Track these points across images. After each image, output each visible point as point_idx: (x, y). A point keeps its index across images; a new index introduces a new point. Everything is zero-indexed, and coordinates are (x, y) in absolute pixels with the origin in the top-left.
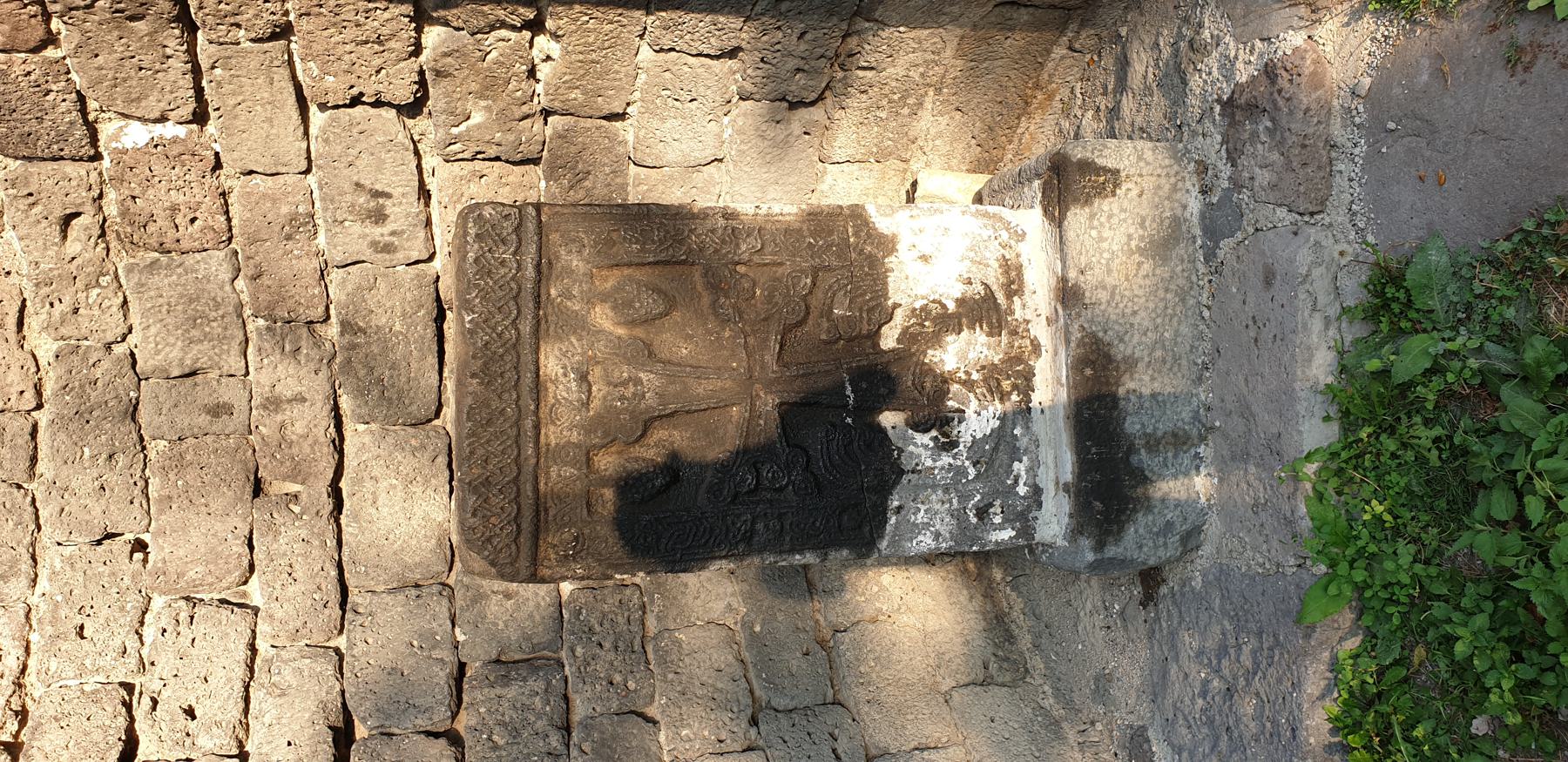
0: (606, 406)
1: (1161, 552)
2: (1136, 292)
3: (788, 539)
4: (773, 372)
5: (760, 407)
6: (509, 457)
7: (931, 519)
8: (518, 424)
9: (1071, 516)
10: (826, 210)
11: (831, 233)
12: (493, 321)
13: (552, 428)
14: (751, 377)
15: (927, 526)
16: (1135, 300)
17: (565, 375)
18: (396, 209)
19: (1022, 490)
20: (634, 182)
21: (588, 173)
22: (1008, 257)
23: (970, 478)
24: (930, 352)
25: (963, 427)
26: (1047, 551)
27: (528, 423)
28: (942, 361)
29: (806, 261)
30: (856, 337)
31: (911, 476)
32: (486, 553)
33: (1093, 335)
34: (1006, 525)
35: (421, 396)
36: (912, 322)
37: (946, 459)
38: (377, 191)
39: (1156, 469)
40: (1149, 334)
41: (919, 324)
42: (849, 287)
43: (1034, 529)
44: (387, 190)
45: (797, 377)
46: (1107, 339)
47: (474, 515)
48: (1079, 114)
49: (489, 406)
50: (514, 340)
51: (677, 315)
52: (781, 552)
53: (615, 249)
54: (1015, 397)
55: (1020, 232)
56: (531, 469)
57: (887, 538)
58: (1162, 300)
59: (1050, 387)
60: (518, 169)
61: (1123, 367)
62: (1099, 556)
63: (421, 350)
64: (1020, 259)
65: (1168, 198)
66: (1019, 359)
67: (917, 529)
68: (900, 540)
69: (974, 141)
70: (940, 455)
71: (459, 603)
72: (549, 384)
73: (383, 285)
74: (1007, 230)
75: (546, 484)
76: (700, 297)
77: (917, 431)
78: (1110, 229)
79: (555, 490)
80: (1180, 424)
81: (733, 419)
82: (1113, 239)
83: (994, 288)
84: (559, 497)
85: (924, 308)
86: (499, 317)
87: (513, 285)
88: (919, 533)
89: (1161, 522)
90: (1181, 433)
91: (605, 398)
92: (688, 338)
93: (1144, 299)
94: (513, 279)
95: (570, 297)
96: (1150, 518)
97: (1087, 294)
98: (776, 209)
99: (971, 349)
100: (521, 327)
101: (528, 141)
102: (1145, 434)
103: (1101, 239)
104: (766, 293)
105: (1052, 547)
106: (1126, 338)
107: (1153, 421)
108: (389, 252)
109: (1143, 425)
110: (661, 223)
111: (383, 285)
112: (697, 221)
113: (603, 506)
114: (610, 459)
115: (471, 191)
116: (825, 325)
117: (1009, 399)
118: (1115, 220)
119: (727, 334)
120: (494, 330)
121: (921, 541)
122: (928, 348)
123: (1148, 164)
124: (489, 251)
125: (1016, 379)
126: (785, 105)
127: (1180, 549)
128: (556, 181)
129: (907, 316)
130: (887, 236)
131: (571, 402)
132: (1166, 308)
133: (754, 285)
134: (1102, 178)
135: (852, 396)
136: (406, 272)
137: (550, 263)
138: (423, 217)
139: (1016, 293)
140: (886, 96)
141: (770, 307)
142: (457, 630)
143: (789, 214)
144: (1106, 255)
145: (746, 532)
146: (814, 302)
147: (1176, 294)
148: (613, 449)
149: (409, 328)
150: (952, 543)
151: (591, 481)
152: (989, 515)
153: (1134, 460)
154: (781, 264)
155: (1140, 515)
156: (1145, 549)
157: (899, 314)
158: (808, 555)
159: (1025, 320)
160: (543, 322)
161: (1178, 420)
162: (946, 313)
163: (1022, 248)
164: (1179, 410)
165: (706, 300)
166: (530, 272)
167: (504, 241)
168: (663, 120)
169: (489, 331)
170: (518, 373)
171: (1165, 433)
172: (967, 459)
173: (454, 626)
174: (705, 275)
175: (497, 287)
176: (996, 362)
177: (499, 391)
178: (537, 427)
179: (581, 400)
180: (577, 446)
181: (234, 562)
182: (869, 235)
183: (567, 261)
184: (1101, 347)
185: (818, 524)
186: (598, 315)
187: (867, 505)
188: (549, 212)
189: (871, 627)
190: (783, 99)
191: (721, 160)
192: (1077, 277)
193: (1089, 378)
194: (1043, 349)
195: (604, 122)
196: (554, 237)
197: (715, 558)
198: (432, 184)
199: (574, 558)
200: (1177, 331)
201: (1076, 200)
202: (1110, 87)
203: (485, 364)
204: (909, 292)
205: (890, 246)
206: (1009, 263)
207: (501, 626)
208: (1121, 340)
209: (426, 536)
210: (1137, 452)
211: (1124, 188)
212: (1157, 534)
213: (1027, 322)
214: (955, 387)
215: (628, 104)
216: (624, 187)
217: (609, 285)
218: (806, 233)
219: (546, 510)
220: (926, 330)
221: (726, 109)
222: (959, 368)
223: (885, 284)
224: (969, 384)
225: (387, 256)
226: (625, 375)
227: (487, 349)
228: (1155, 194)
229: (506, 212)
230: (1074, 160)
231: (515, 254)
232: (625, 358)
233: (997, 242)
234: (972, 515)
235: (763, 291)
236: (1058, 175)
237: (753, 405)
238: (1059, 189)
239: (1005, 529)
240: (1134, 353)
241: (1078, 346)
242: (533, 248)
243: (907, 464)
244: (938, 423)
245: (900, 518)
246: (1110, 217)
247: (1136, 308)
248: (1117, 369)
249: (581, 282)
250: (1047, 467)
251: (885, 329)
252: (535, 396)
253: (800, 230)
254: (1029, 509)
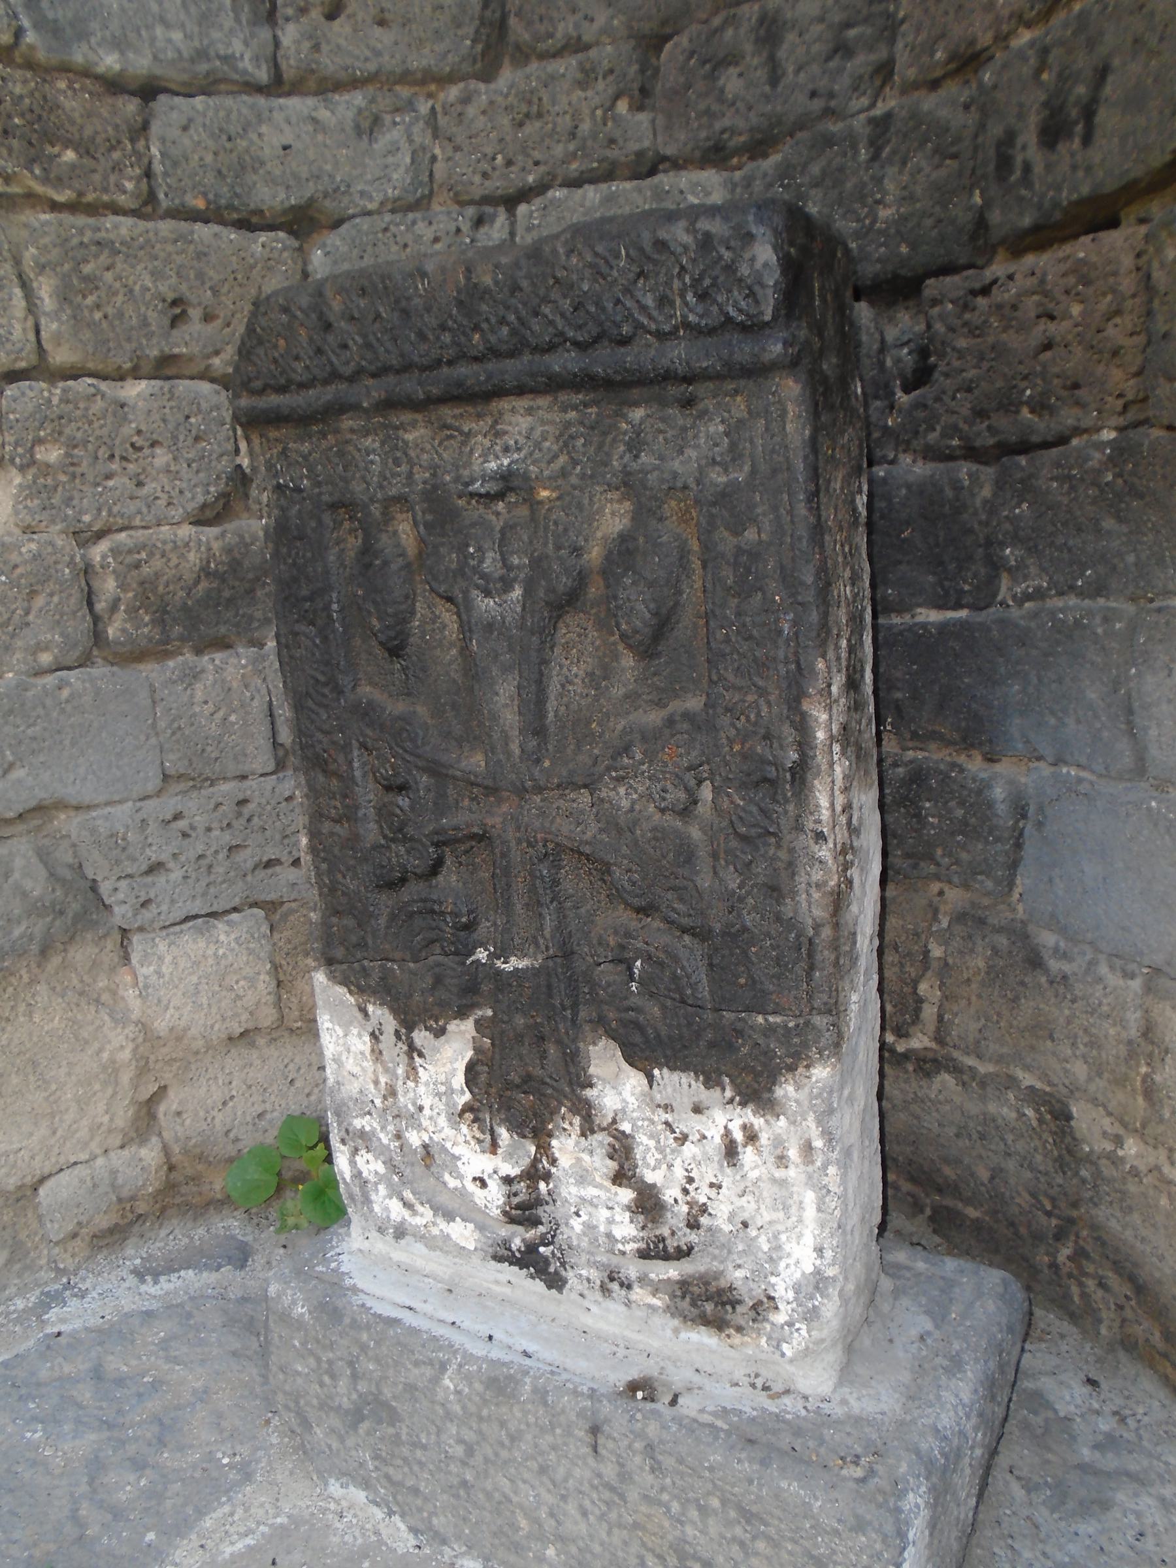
86: (566, 304)
94: (639, 326)
103: (703, 1510)
108: (999, 168)
120: (546, 300)
128: (1110, 458)
135: (508, 967)
144: (675, 1507)
179: (473, 481)
181: (542, 28)
231: (686, 325)
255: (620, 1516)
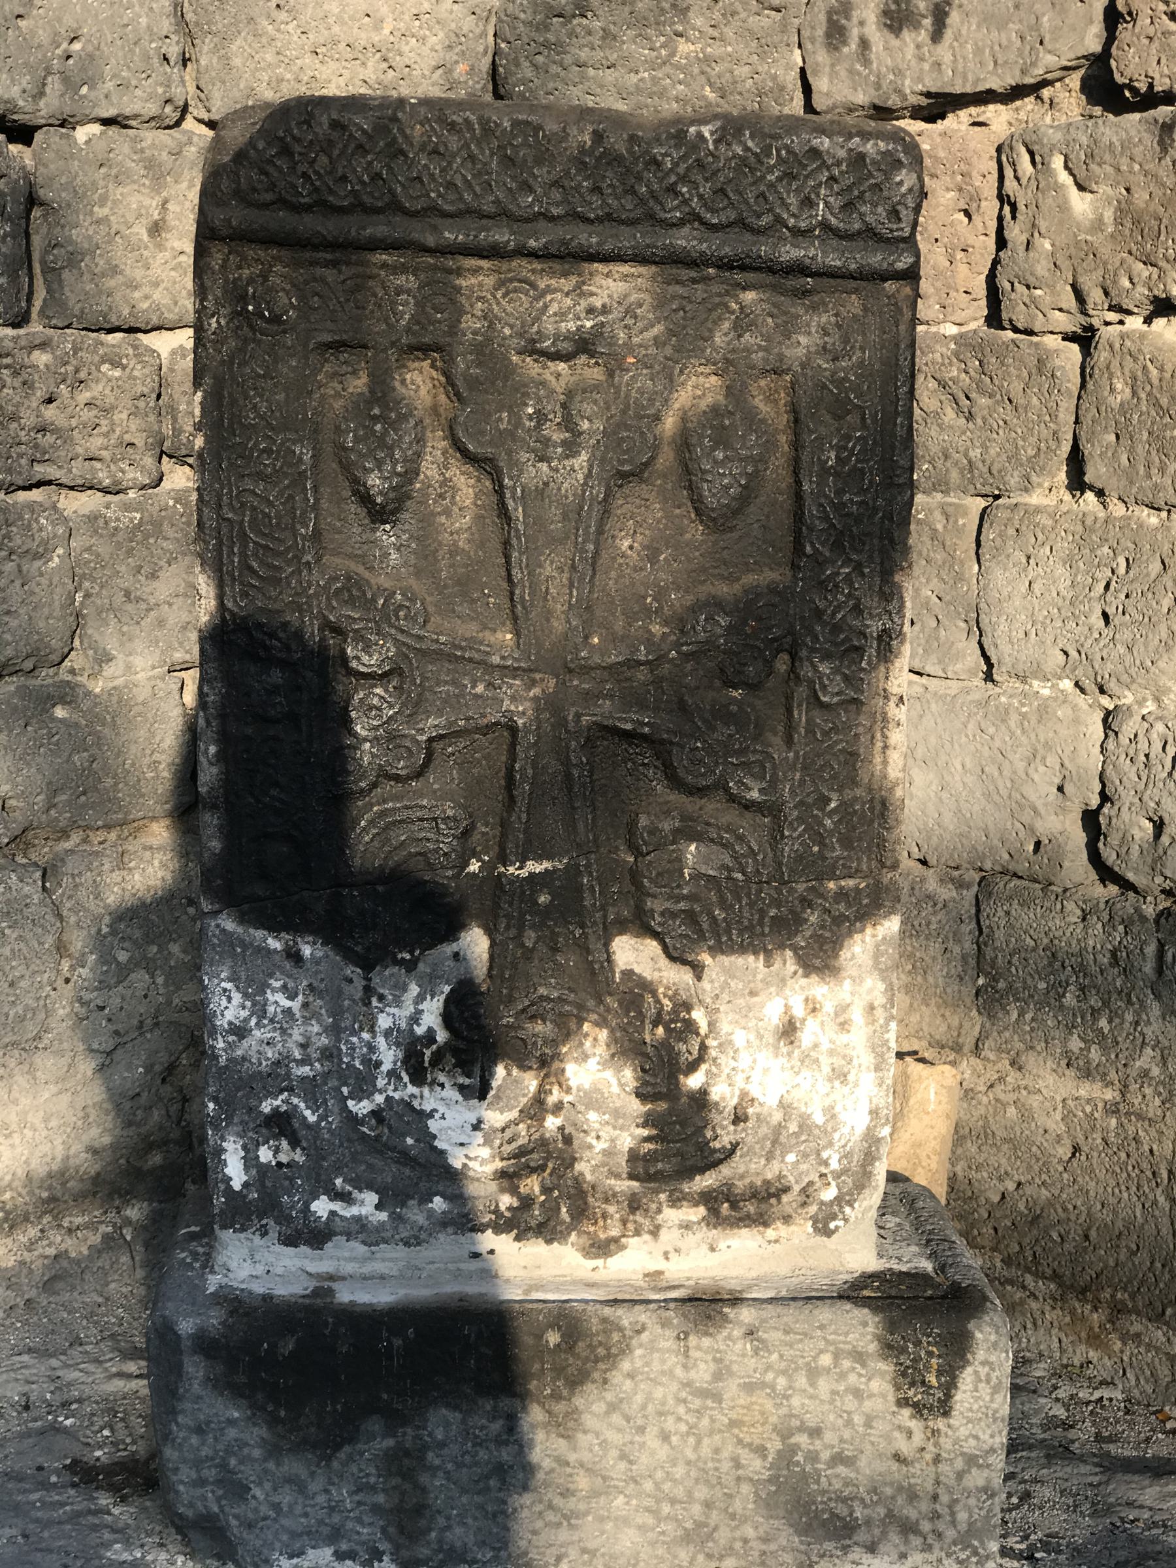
0: (526, 385)
1: (186, 1473)
2: (706, 1441)
3: (249, 731)
4: (578, 716)
5: (511, 686)
6: (440, 195)
7: (272, 1021)
8: (503, 215)
9: (267, 1298)
10: (892, 837)
11: (846, 843)
12: (699, 178)
13: (490, 281)
14: (570, 671)
15: (260, 1011)
16: (692, 1440)
17: (590, 311)
18: (910, 51)
19: (322, 1207)
20: (950, 504)
21: (970, 417)
22: (785, 1199)
23: (350, 1103)
24: (603, 1035)
25: (451, 1093)
26: (197, 1260)
27: (503, 236)
28: (585, 1057)
29: (792, 791)
30: (639, 886)
31: (359, 983)
32: (261, 145)
33: (626, 1350)
34: (254, 1172)
35: (551, 85)
36: (666, 1002)
37: (388, 1056)
38: (946, 14)
39: (354, 1469)
40: (623, 1465)
41: (659, 1014)
42: (739, 876)
43: (243, 1230)
44: (948, 34)
45: (567, 763)
46: (616, 1377)
47: (335, 125)
48: (1061, 1394)
49: (539, 162)
50: (663, 215)
51: (696, 532)
52: (223, 716)
53: (828, 418)
54: (506, 1201)
55: (832, 1225)
56: (415, 236)
57: (240, 930)
58: (690, 1494)
59: (522, 1273)
60: (981, 291)
61: (560, 1408)
62: (186, 1344)
63: (638, 90)
64: (779, 1224)
65: (890, 1514)
66: (581, 1212)
67: (254, 990)
68: (234, 955)
69: (1011, 1186)
70: (398, 1045)
71: (150, 136)
72: (574, 280)
73: (765, 22)
74: (839, 1200)
75: (384, 265)
76: (731, 579)
77: (447, 1001)
78: (834, 1393)
79: (371, 283)
80: (441, 1521)
81: (487, 633)
82: (811, 1397)
83: (725, 1170)
84: (358, 288)
85: (690, 1027)
86: (706, 189)
87: (765, 221)
88: (246, 996)
89: (248, 1473)
90: (423, 1523)
91: (543, 383)
92: (651, 552)
93: (690, 1454)
94: (779, 220)
95: (739, 328)
96: (257, 1453)
97: (706, 1342)
98: (896, 737)
99: (607, 1117)
100: (686, 230)
101: (1034, 300)
102: (425, 1448)
103: (814, 1373)
104: (733, 708)
105: (204, 1267)
106: (616, 1418)
107: (450, 1466)
108: (828, 35)
109: (442, 1445)
110: (875, 510)
111: (765, 22)
112: (877, 580)
113: (335, 374)
114: (423, 392)
115: (940, 192)
116: (666, 826)
117: (502, 1190)
118: (850, 1403)
119: (657, 629)
120: (683, 179)
121: (229, 999)
122: (612, 1031)
123: (960, 1476)
124: (832, 178)
125: (542, 1204)
126: (1095, 801)
127: (190, 1513)
128: (957, 354)
129: (676, 993)
130: (836, 956)
131: (537, 319)
132: (673, 1501)
133: (753, 687)
134: (932, 1379)
135: (524, 873)
136: (789, 67)
137: (805, 293)
138: (893, 101)
139: (714, 1211)
140: (1106, 1004)
141: (707, 715)
142: (96, 128)
143: (885, 763)
144: (782, 1382)
145: (267, 648)
146: (711, 808)
147: (699, 1525)
148: (442, 398)
149: (678, 67)
150: (223, 1061)
151: (385, 350)
152: (276, 1137)
153: (374, 1424)
154: (789, 741)
155: (260, 1431)
156: (194, 1440)
157: (684, 976)
158: (214, 770)
159: (658, 1228)
160: (693, 274)
161: (448, 1518)
162: (679, 1070)
163: (802, 1230)
164: (470, 1521)
165: (723, 590)
166: (790, 253)
167: (848, 206)
168: (1069, 562)
169: (682, 169)
170: (600, 220)
171: (424, 1490)
172: (389, 1099)
173: (107, 122)
174: (773, 589)
175: (762, 188)
176: (580, 1167)
177: (566, 183)
178: (494, 252)
180: (454, 329)
182: (839, 920)
183: (808, 325)
184: (601, 1366)
185: (274, 792)
186: (702, 379)
187: (305, 894)
188: (903, 294)
189: (49, 941)
190: (1105, 797)
191: (989, 677)
192: (740, 1323)
193: (539, 1337)
194: (599, 1262)
195: (1066, 447)
196: (854, 304)
197: (220, 587)
198: (957, 122)
199: (239, 314)
200: (626, 1521)
201: (891, 1326)
202: (1113, 1449)
203: (618, 159)
204: (725, 997)
205: (817, 962)
206: (773, 1201)
207: (100, 212)
208: (612, 1408)
209: (280, 80)
210: (390, 1432)
211: (915, 1425)
212: (224, 1466)
213: (655, 1232)
214: (531, 1083)
215: (1100, 493)
216: (943, 486)
217: (759, 402)
218: (848, 794)
219: (335, 264)
220: (648, 1027)
221: (1087, 683)
222: (568, 1090)
223: (743, 949)
224: (537, 1108)
225: (820, 32)
226: (585, 425)
227: (647, 164)
228: (900, 1489)
229: (903, 213)
230: (971, 1326)
231: (825, 226)
232: (618, 425)
233: (814, 1177)
234: (278, 1102)
235: (739, 703)
236: (943, 1297)
237: (515, 672)
238: (916, 1298)
239: (246, 1168)
240: (585, 1432)
241: (604, 1320)
242: (834, 261)
243: (383, 977)
244: (462, 1045)
245: (277, 958)
246: (857, 1393)
247: (674, 1439)
248: (556, 1396)
249: (766, 350)
250: (365, 1260)
251: (652, 946)
252: (553, 250)
253: (854, 782)
254: (283, 1218)
255: (713, 1420)
